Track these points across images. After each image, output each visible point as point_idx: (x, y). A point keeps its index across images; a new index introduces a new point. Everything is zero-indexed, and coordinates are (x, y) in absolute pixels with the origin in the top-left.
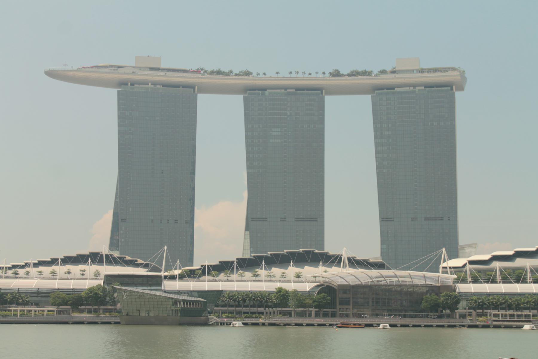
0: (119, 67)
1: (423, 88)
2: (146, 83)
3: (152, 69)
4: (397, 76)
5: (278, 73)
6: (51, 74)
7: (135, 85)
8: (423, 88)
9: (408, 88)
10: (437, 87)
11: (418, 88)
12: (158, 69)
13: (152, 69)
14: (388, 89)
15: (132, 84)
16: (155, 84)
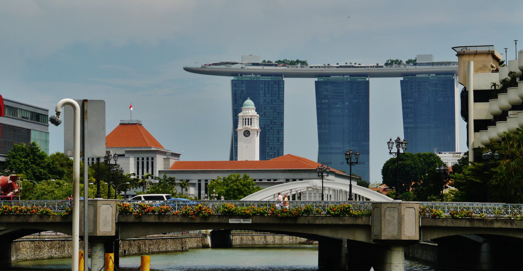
0: (233, 64)
1: (434, 75)
2: (250, 73)
3: (254, 64)
4: (417, 67)
5: (338, 64)
6: (187, 69)
7: (243, 76)
8: (434, 75)
9: (424, 75)
10: (444, 74)
11: (431, 75)
12: (257, 64)
13: (254, 64)
14: (411, 75)
15: (241, 75)
16: (256, 74)
